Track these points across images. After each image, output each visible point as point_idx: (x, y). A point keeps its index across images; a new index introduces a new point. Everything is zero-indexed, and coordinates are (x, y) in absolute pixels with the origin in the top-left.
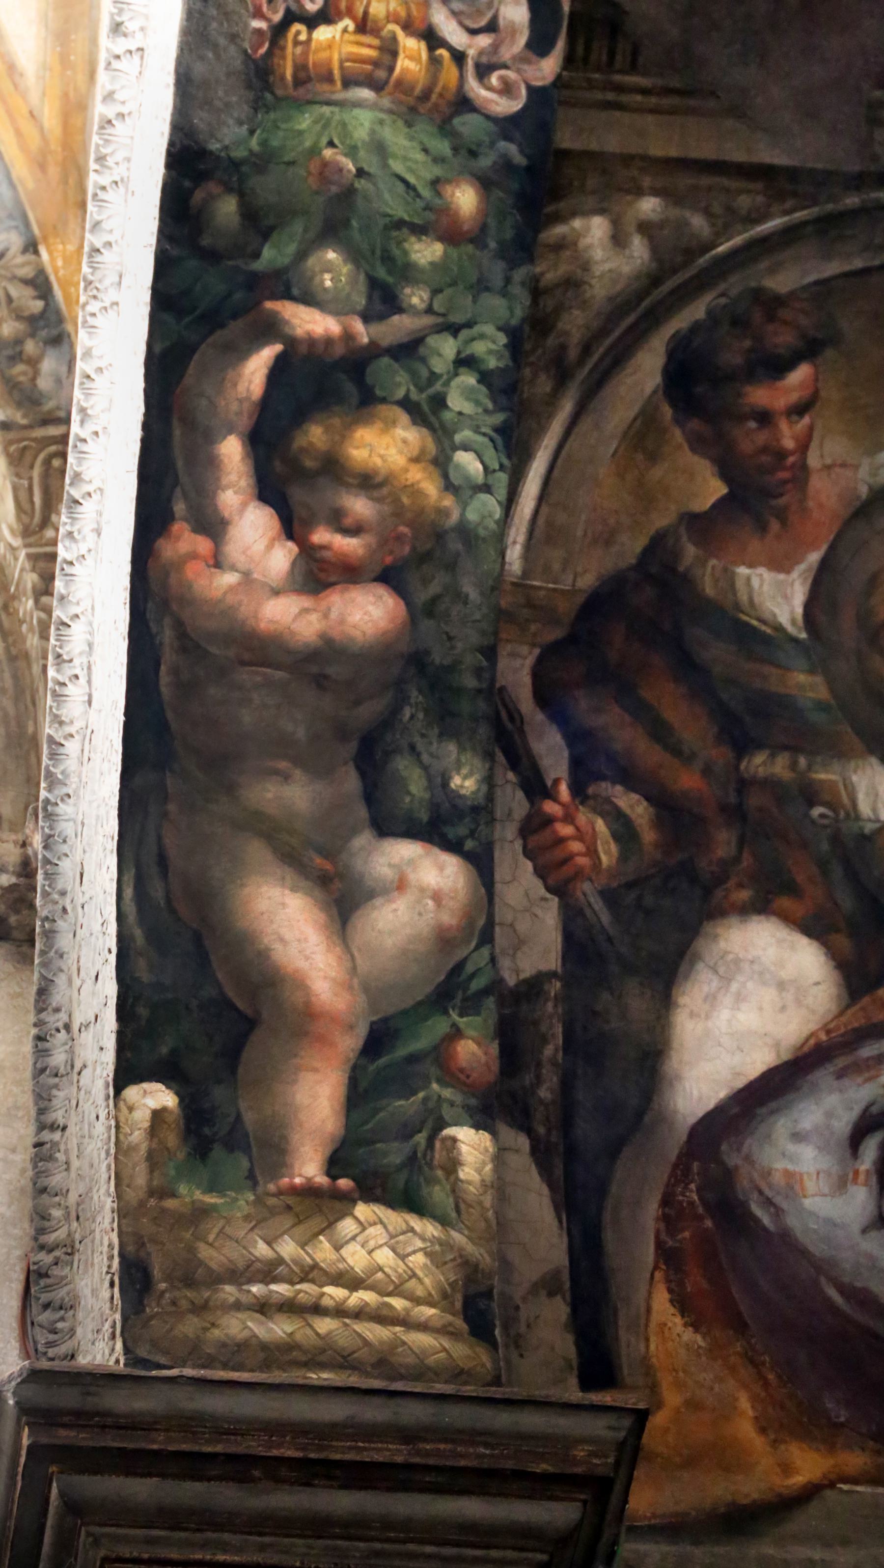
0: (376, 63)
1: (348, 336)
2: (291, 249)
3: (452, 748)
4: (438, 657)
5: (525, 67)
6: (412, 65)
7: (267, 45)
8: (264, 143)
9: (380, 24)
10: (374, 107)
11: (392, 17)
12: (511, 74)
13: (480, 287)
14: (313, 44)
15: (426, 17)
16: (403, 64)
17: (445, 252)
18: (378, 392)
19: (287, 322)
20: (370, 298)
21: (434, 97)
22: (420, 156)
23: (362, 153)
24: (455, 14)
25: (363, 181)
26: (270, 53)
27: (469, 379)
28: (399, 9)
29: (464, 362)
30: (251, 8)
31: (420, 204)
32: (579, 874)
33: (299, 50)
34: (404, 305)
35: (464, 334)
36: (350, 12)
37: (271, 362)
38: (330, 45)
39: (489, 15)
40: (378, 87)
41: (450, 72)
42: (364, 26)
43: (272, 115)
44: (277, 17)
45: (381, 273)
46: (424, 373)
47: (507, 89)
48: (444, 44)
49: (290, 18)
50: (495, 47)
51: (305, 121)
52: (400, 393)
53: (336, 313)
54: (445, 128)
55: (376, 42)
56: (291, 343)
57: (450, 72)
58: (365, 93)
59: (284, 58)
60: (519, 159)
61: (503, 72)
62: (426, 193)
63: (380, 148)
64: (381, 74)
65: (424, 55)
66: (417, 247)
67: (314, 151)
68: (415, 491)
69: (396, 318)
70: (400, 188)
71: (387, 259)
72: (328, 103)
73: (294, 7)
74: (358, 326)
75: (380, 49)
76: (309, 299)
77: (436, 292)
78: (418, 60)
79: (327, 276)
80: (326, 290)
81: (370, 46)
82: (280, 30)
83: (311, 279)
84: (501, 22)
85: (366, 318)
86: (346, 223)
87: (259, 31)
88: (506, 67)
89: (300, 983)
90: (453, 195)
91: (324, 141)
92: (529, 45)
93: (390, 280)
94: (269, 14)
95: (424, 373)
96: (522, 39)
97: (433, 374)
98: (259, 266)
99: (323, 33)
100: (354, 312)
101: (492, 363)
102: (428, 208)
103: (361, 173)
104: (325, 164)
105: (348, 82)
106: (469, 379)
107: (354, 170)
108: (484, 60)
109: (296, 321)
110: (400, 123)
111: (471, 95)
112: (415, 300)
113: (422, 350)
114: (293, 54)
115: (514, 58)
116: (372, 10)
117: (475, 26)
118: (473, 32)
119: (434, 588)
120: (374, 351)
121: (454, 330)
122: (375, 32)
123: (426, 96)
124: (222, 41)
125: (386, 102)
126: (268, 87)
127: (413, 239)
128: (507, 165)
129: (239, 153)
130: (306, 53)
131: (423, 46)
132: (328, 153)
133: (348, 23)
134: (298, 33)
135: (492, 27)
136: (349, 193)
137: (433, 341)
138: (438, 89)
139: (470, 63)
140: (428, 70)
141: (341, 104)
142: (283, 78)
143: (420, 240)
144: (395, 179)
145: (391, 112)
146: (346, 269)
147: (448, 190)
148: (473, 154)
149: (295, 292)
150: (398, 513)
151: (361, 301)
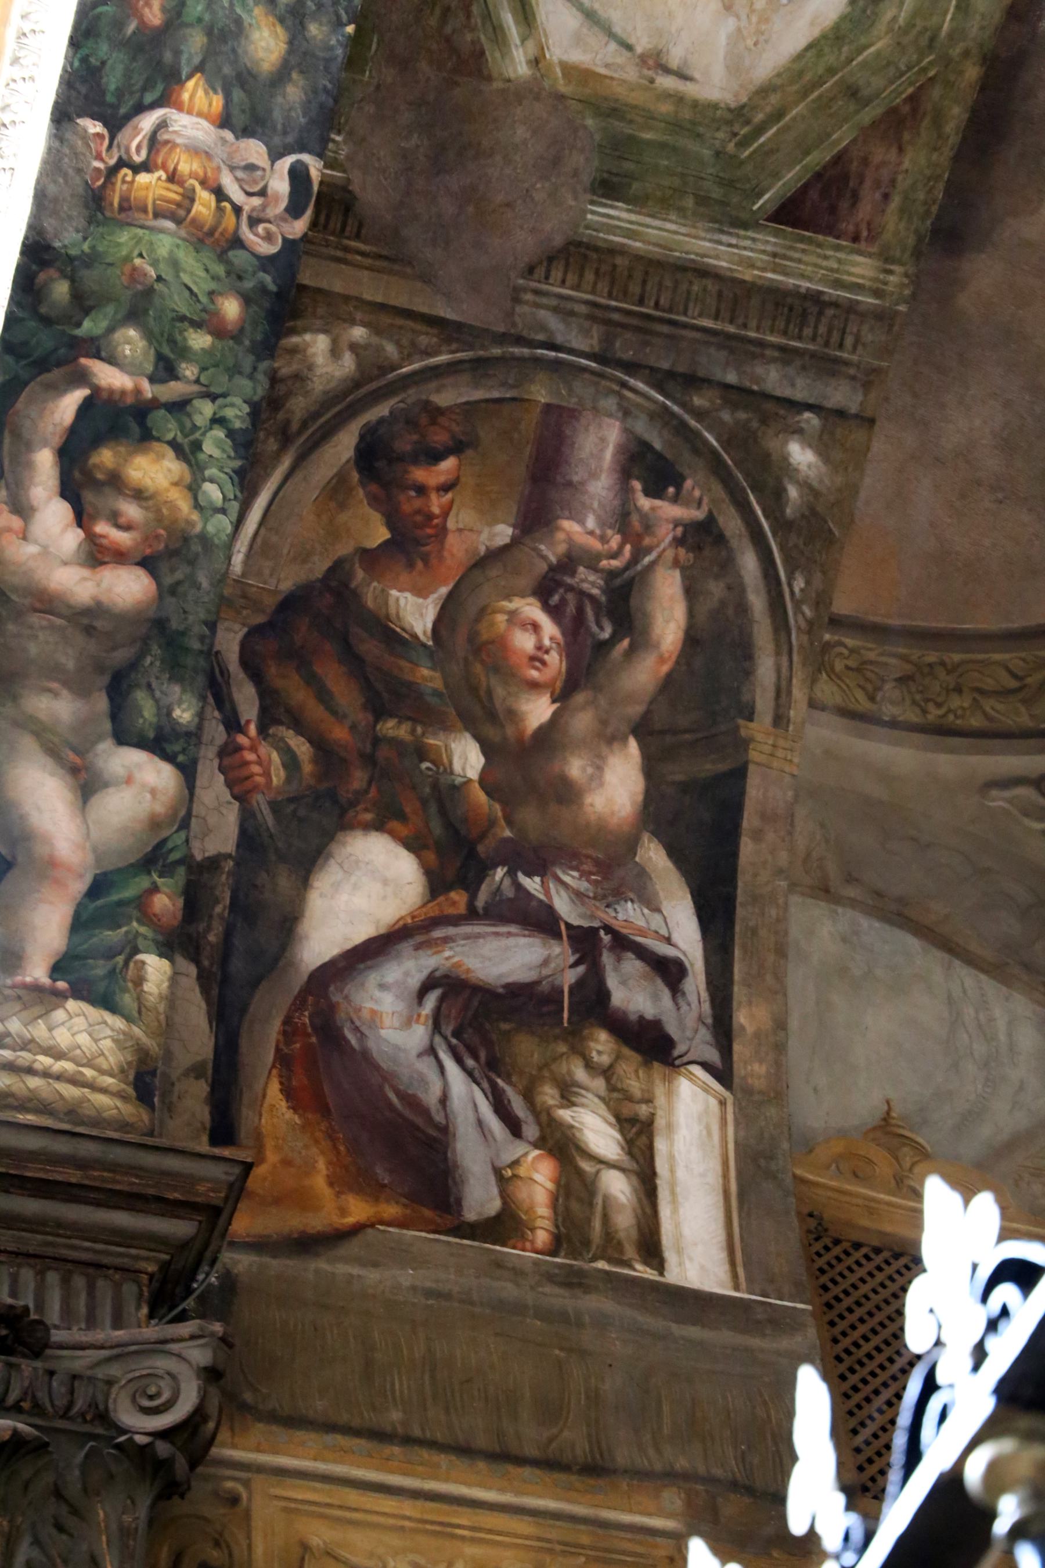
0: (179, 205)
1: (138, 391)
2: (104, 324)
3: (177, 689)
4: (174, 625)
6: (203, 210)
7: (102, 180)
8: (93, 248)
9: (185, 178)
11: (193, 175)
12: (273, 228)
13: (234, 371)
14: (136, 184)
15: (217, 179)
16: (198, 208)
17: (213, 343)
18: (154, 433)
19: (95, 375)
21: (217, 235)
22: (203, 274)
23: (162, 266)
24: (237, 179)
25: (160, 285)
26: (104, 186)
27: (219, 433)
29: (217, 421)
30: (94, 153)
31: (199, 307)
32: (256, 788)
33: (125, 187)
34: (180, 375)
36: (164, 167)
37: (80, 401)
38: (147, 188)
39: (261, 184)
40: (179, 222)
41: (230, 220)
42: (173, 178)
43: (101, 229)
44: (112, 162)
45: (166, 350)
46: (188, 425)
47: (269, 237)
48: (228, 199)
49: (121, 163)
50: (264, 207)
51: (124, 237)
52: (170, 436)
54: (222, 257)
55: (180, 190)
56: (96, 390)
57: (230, 220)
58: (169, 225)
59: (114, 191)
60: (272, 287)
61: (267, 225)
62: (204, 299)
63: (175, 264)
64: (182, 213)
65: (213, 204)
66: (194, 336)
67: (128, 259)
68: (172, 506)
69: (172, 383)
70: (187, 293)
71: (172, 341)
72: (142, 227)
73: (125, 157)
75: (182, 195)
76: (112, 360)
77: (203, 369)
78: (209, 208)
79: (127, 347)
80: (125, 357)
81: (176, 193)
82: (113, 171)
83: (116, 348)
84: (269, 191)
85: (152, 380)
86: (146, 312)
87: (97, 170)
88: (270, 222)
89: (47, 840)
90: (223, 304)
91: (136, 253)
92: (287, 210)
93: (172, 356)
94: (107, 159)
96: (283, 204)
97: (195, 426)
98: (79, 332)
99: (143, 178)
101: (238, 425)
102: (204, 310)
103: (159, 279)
104: (135, 269)
105: (157, 215)
106: (219, 433)
108: (255, 214)
109: (101, 375)
110: (191, 249)
111: (243, 237)
112: (188, 373)
113: (188, 408)
114: (121, 189)
115: (276, 216)
116: (179, 168)
117: (251, 190)
119: (179, 575)
120: (155, 404)
121: (213, 397)
122: (181, 183)
123: (211, 233)
124: (71, 171)
125: (183, 233)
126: (100, 208)
127: (191, 330)
128: (263, 289)
129: (73, 252)
130: (129, 190)
131: (213, 197)
132: (138, 261)
133: (162, 174)
134: (126, 175)
135: (263, 193)
136: (149, 292)
137: (197, 403)
138: (220, 230)
140: (214, 216)
141: (151, 229)
142: (112, 204)
143: (196, 332)
145: (184, 240)
146: (142, 344)
147: (220, 300)
148: (240, 278)
149: (103, 354)
150: (159, 519)
151: (149, 368)
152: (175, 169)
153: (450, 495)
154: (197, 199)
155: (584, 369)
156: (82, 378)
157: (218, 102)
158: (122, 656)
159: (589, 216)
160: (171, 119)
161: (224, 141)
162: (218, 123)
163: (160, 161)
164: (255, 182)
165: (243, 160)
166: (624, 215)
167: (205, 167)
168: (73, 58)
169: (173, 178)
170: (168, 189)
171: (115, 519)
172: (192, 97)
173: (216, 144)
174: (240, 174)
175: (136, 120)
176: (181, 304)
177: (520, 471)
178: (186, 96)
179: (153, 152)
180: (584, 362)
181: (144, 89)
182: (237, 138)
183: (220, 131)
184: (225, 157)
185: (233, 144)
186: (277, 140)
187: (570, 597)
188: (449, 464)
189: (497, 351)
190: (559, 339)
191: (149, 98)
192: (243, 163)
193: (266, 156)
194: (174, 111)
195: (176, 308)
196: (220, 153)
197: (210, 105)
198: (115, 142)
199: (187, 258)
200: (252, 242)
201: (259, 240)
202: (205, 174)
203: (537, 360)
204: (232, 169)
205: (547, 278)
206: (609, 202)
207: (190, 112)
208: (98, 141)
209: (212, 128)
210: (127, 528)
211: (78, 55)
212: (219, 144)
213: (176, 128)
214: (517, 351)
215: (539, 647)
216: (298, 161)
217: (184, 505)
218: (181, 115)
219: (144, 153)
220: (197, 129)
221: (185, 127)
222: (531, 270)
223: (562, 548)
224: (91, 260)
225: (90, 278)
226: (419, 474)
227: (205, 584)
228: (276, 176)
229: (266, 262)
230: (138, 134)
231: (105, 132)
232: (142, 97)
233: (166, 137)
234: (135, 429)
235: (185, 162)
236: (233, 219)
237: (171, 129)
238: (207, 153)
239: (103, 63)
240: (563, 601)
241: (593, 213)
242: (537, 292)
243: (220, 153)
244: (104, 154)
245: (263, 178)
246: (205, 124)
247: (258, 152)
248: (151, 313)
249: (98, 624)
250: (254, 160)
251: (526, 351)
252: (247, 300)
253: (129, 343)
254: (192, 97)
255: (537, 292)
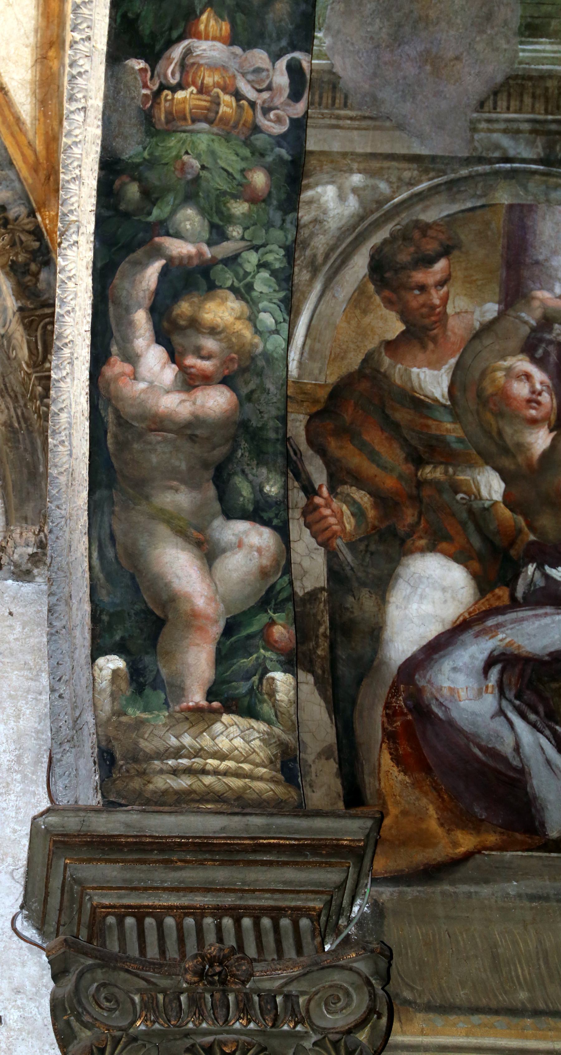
0: (208, 109)
1: (200, 254)
2: (168, 209)
3: (264, 470)
4: (254, 423)
5: (288, 108)
6: (228, 110)
7: (150, 102)
8: (151, 154)
9: (210, 89)
10: (208, 133)
11: (216, 85)
13: (269, 225)
14: (175, 101)
15: (234, 84)
16: (223, 109)
17: (250, 207)
18: (217, 283)
19: (168, 248)
20: (211, 233)
21: (240, 126)
22: (235, 158)
23: (203, 157)
24: (249, 81)
25: (204, 172)
26: (152, 106)
27: (264, 274)
28: (220, 80)
29: (262, 265)
31: (235, 182)
32: (334, 535)
33: (168, 104)
34: (229, 237)
35: (262, 250)
36: (194, 84)
37: (159, 270)
38: (184, 100)
39: (267, 82)
40: (211, 122)
42: (202, 90)
44: (155, 88)
45: (216, 220)
46: (241, 273)
47: (279, 120)
49: (162, 87)
50: (272, 98)
51: (172, 142)
52: (229, 283)
53: (193, 242)
54: (247, 143)
55: (208, 98)
56: (170, 260)
58: (204, 126)
59: (160, 109)
60: (287, 157)
62: (238, 176)
63: (213, 153)
64: (212, 115)
65: (234, 104)
66: (234, 205)
67: (178, 157)
68: (239, 335)
69: (225, 244)
70: (225, 174)
71: (219, 212)
72: (184, 131)
73: (164, 82)
74: (205, 248)
75: (211, 102)
76: (178, 235)
77: (245, 229)
78: (231, 107)
79: (188, 223)
80: (187, 230)
81: (205, 101)
82: (157, 94)
84: (274, 85)
85: (210, 244)
86: (197, 195)
87: (146, 95)
88: (278, 109)
89: (188, 598)
91: (183, 151)
93: (221, 223)
95: (241, 273)
97: (246, 272)
98: (151, 219)
99: (180, 95)
100: (202, 241)
101: (277, 265)
102: (240, 184)
103: (203, 167)
104: (184, 164)
105: (194, 121)
106: (264, 274)
107: (199, 167)
108: (266, 105)
109: (172, 248)
110: (223, 140)
112: (235, 234)
113: (239, 260)
114: (165, 107)
115: (282, 103)
116: (205, 82)
117: (261, 88)
118: (260, 91)
119: (252, 386)
120: (214, 262)
121: (256, 248)
122: (208, 93)
123: (236, 126)
127: (232, 201)
129: (137, 160)
130: (172, 105)
131: (233, 99)
132: (185, 158)
133: (193, 89)
134: (167, 95)
135: (269, 88)
138: (242, 122)
139: (259, 107)
140: (236, 112)
142: (160, 119)
143: (236, 202)
144: (221, 171)
145: (217, 134)
148: (262, 155)
149: (171, 231)
151: (206, 235)
152: (202, 83)
153: (445, 289)
154: (222, 102)
155: (534, 172)
156: (158, 252)
157: (225, 27)
158: (219, 453)
159: (521, 54)
160: (193, 47)
161: (235, 55)
162: (229, 42)
163: (190, 79)
164: (263, 81)
165: (251, 66)
166: (548, 47)
167: (224, 77)
168: (116, 15)
169: (202, 90)
170: (199, 99)
171: (199, 352)
172: (207, 26)
173: (229, 59)
174: (250, 77)
175: (167, 54)
176: (222, 184)
177: (496, 259)
178: (202, 27)
179: (184, 74)
180: (534, 167)
181: (171, 29)
182: (244, 50)
183: (231, 48)
184: (237, 66)
185: (241, 57)
186: (275, 48)
187: (551, 349)
188: (441, 264)
189: (464, 172)
190: (512, 153)
191: (175, 34)
192: (252, 69)
193: (268, 60)
194: (195, 40)
195: (219, 187)
196: (233, 65)
197: (221, 30)
198: (156, 72)
199: (222, 149)
200: (268, 126)
201: (272, 124)
202: (225, 82)
203: (496, 173)
204: (244, 75)
205: (495, 108)
206: (535, 40)
207: (207, 39)
208: (143, 74)
209: (225, 47)
210: (208, 357)
211: (119, 14)
212: (232, 57)
213: (199, 53)
214: (480, 168)
215: (533, 392)
216: (293, 59)
217: (248, 333)
218: (201, 42)
219: (178, 76)
220: (214, 50)
221: (205, 50)
222: (482, 104)
223: (538, 313)
224: (152, 163)
225: (153, 177)
226: (419, 276)
227: (272, 388)
228: (278, 73)
229: (280, 139)
230: (171, 63)
231: (148, 67)
232: (170, 35)
233: (192, 61)
234: (203, 283)
235: (209, 76)
236: (250, 112)
237: (194, 54)
238: (223, 66)
239: (138, 15)
240: (546, 354)
241: (524, 51)
242: (489, 121)
243: (233, 65)
244: (149, 84)
245: (268, 76)
246: (218, 45)
247: (261, 58)
248: (201, 194)
249: (198, 432)
250: (260, 64)
251: (487, 168)
252: (270, 171)
253: (188, 220)
254: (207, 26)
255: (489, 121)
